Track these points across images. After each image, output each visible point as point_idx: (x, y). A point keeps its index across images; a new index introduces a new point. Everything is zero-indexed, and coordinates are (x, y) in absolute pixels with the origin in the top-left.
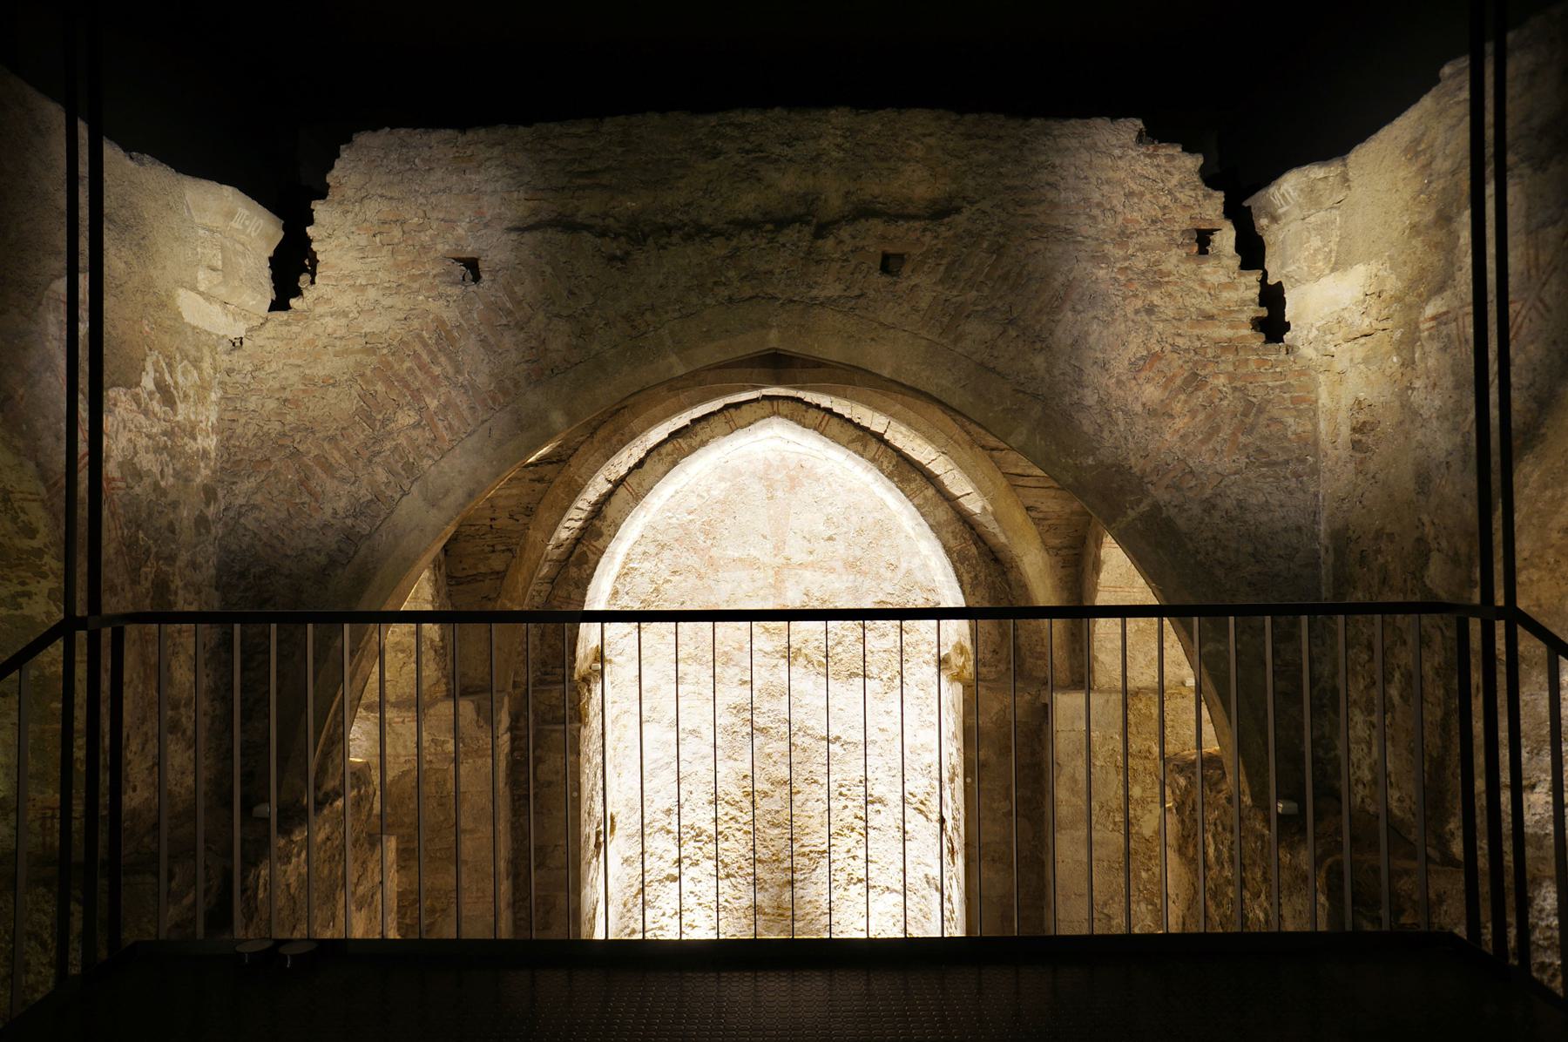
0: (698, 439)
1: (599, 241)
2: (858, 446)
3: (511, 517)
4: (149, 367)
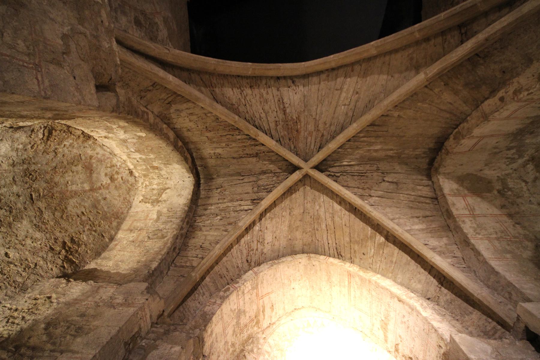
0: (281, 261)
3: (210, 244)
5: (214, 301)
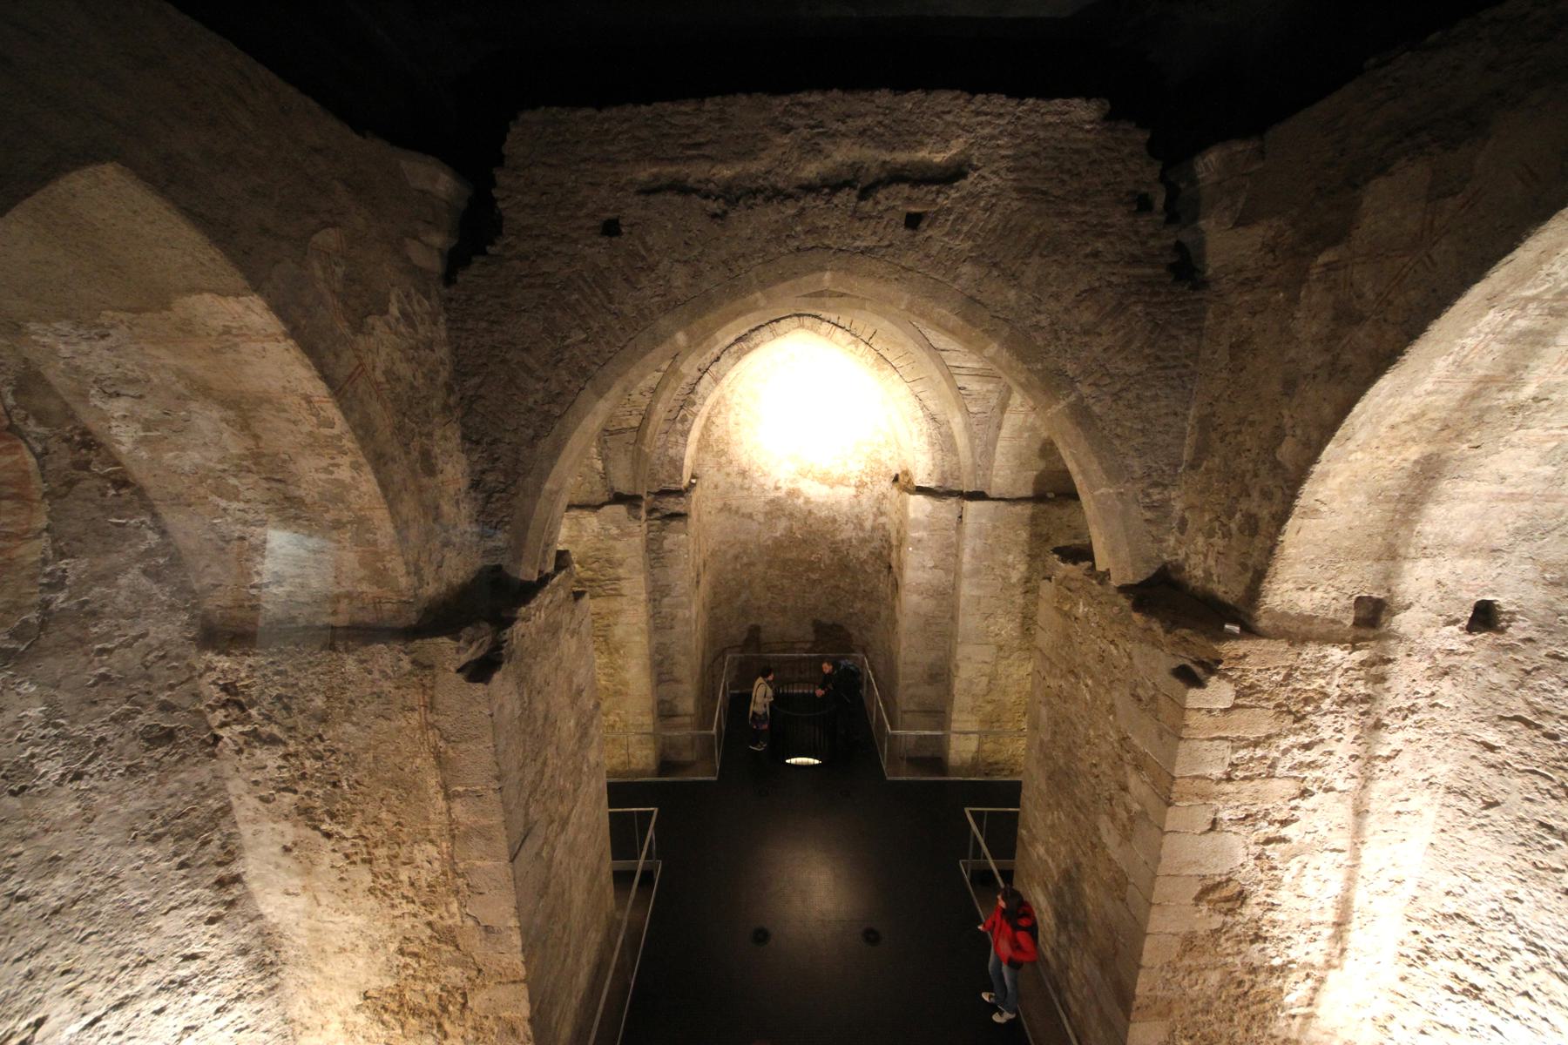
1: (704, 202)
2: (852, 347)
4: (393, 298)
5: (673, 439)
